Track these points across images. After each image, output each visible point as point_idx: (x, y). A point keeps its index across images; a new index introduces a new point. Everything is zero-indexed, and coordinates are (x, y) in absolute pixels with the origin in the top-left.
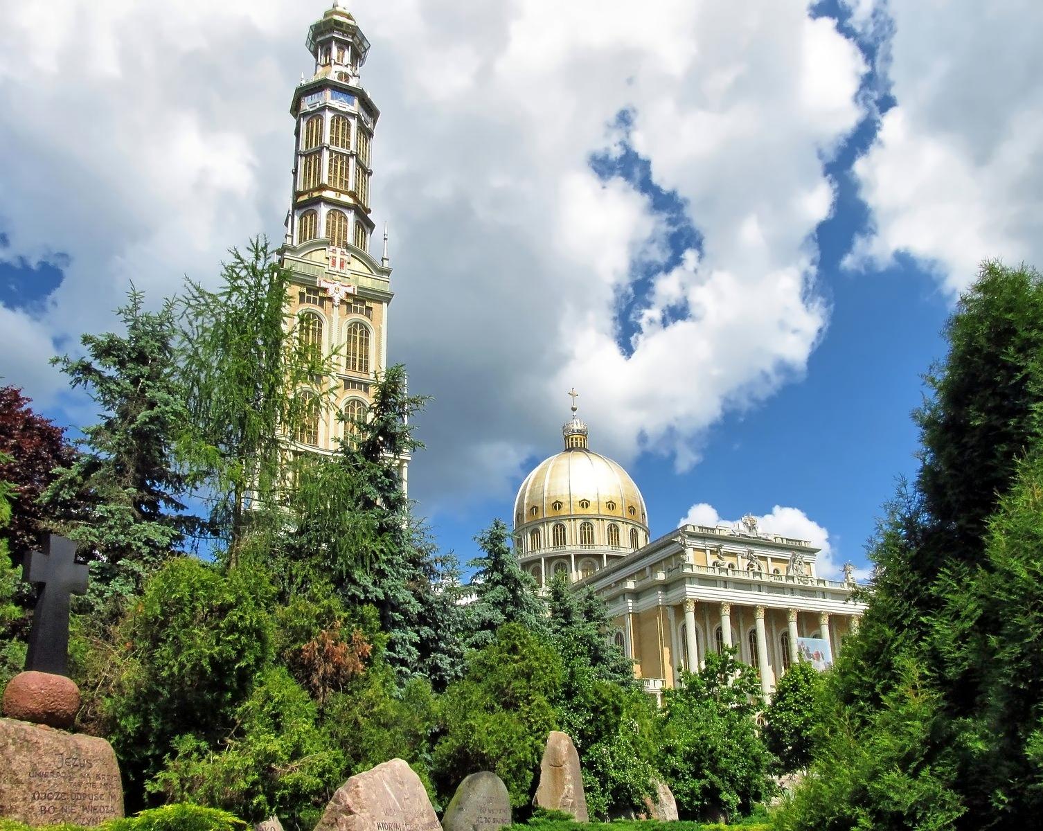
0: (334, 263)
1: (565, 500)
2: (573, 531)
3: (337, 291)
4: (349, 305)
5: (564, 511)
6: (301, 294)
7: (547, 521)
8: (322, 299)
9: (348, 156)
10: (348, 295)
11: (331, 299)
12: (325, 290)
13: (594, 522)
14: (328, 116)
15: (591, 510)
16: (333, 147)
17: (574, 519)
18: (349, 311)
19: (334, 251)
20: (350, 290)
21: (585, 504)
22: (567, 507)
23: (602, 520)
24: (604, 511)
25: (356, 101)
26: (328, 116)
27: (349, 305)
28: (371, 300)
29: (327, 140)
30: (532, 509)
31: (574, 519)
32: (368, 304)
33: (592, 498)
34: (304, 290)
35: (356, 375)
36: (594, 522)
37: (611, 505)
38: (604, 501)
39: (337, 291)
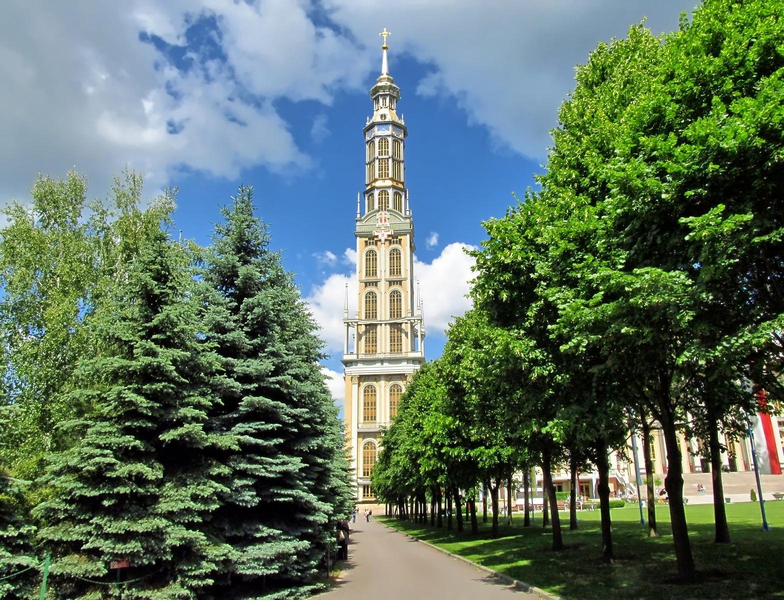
0: (381, 221)
3: (383, 235)
4: (390, 241)
6: (366, 242)
8: (376, 241)
9: (388, 159)
10: (389, 236)
11: (380, 240)
12: (377, 236)
14: (377, 140)
16: (381, 157)
18: (390, 243)
19: (381, 214)
20: (389, 233)
25: (390, 127)
26: (377, 140)
27: (390, 241)
28: (401, 235)
29: (377, 155)
32: (399, 238)
34: (367, 239)
35: (394, 278)
39: (383, 235)
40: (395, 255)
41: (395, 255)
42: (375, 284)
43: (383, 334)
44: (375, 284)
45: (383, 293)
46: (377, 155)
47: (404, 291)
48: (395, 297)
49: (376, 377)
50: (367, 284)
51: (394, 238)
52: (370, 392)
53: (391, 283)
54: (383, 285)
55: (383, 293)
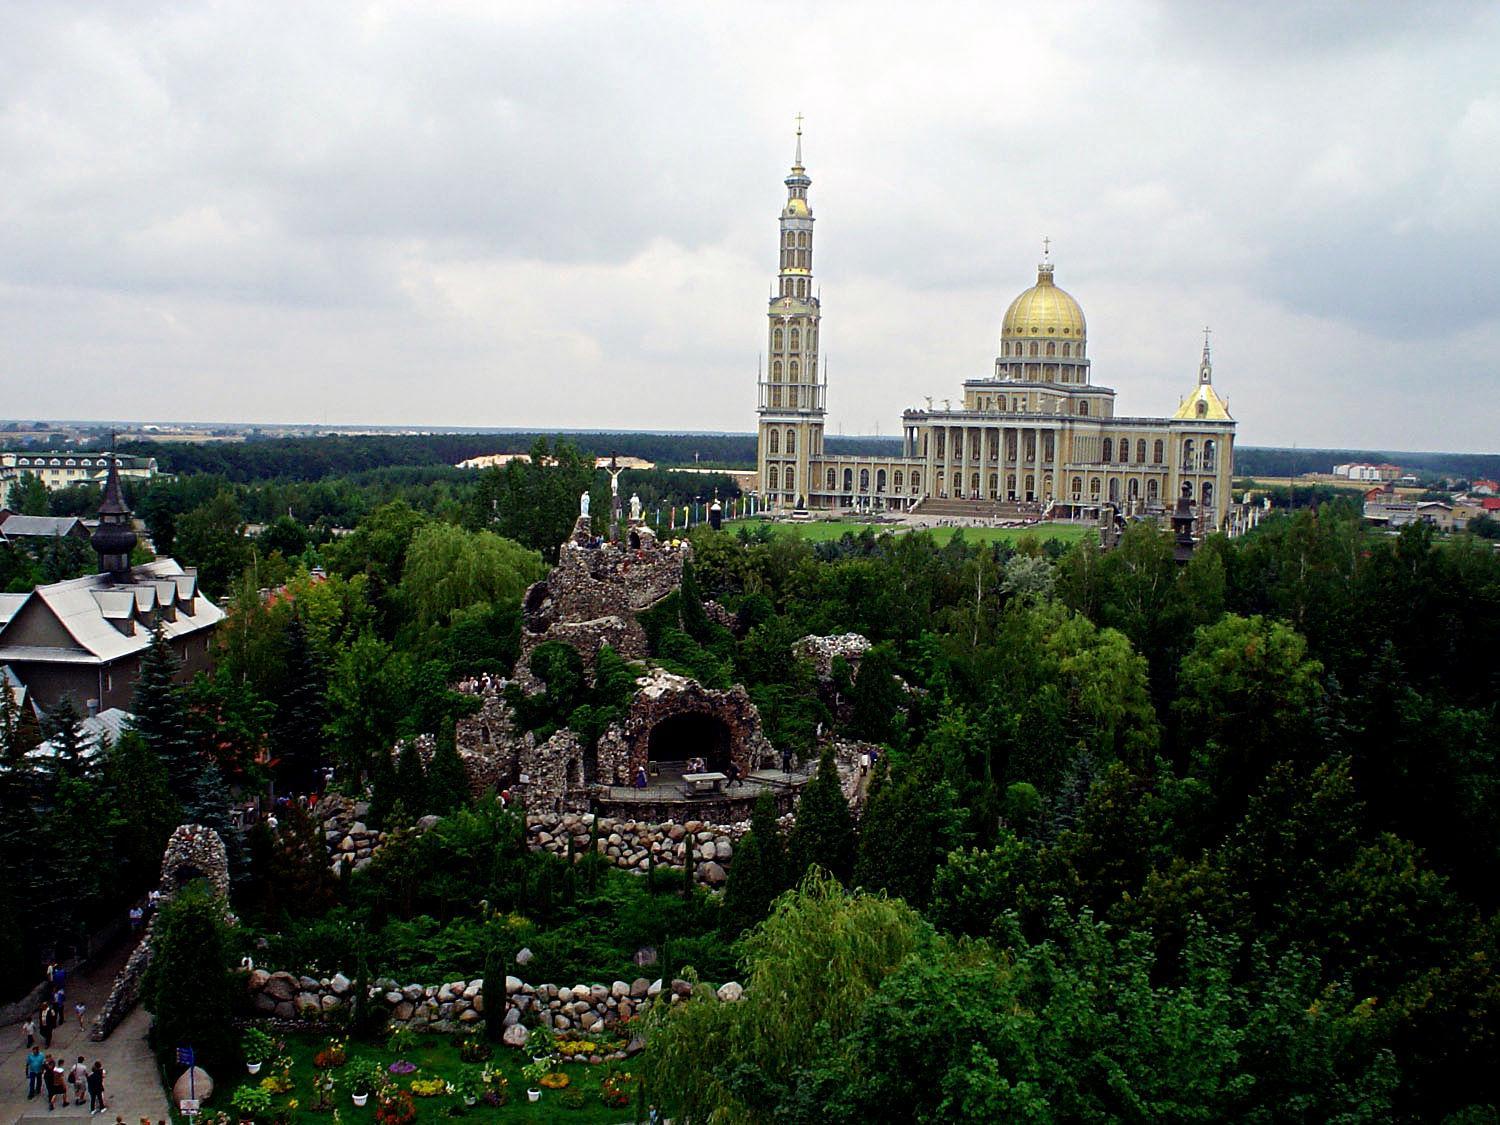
40: (795, 333)
41: (795, 333)
42: (781, 355)
43: (785, 392)
44: (781, 355)
45: (786, 361)
46: (796, 245)
47: (804, 361)
48: (794, 366)
49: (778, 424)
50: (776, 355)
51: (795, 320)
52: (774, 432)
53: (792, 355)
54: (786, 357)
55: (786, 361)
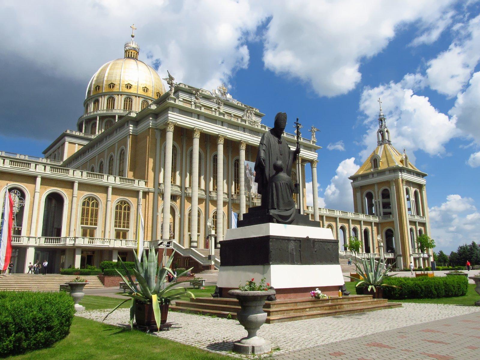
1: (116, 83)
2: (119, 102)
5: (116, 89)
7: (104, 95)
13: (134, 98)
15: (132, 91)
17: (121, 95)
21: (129, 86)
22: (118, 87)
23: (139, 97)
24: (141, 92)
30: (96, 88)
31: (121, 95)
33: (134, 84)
36: (134, 98)
37: (146, 89)
38: (141, 86)
